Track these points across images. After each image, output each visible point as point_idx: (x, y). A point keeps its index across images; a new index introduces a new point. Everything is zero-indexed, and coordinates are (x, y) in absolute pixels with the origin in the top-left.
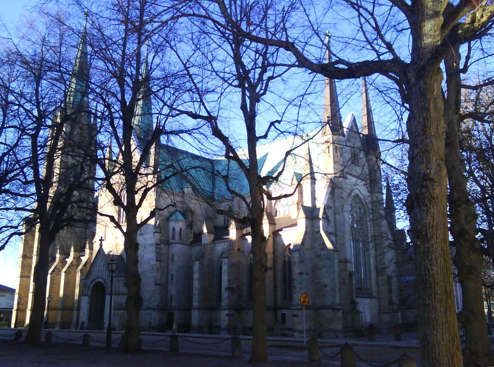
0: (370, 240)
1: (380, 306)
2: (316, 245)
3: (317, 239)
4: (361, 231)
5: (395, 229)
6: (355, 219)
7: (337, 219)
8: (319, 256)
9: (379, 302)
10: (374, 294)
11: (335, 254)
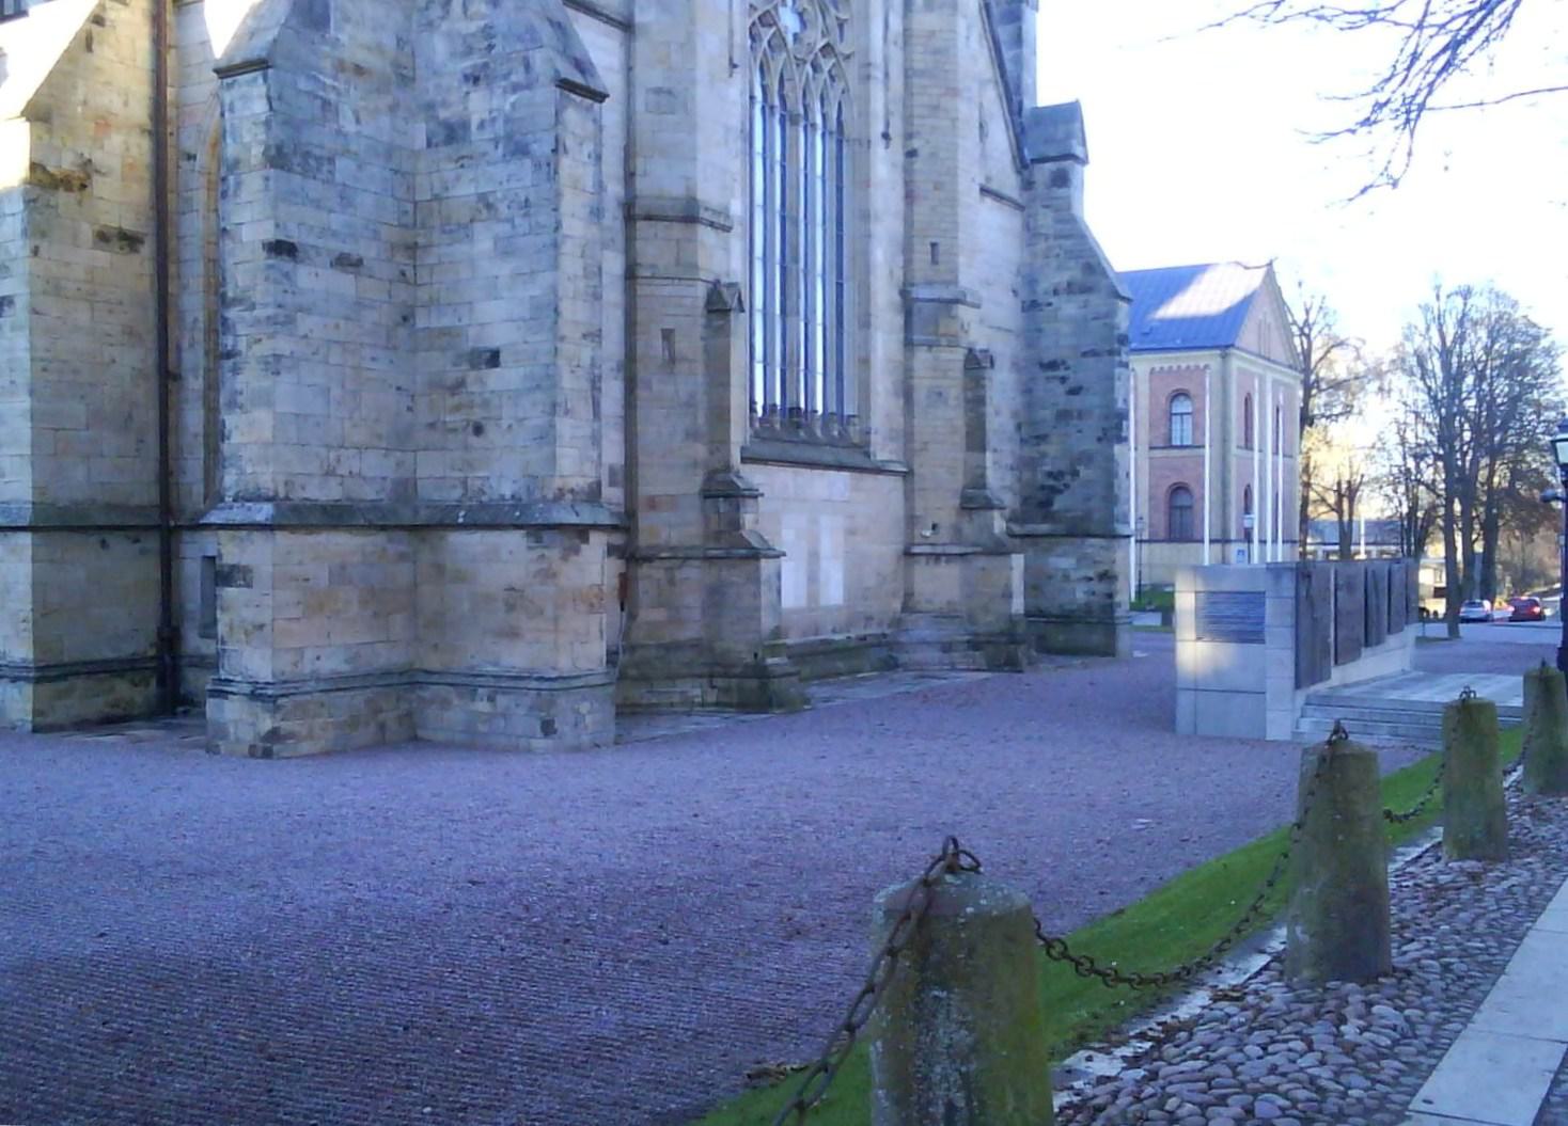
0: (878, 128)
1: (911, 520)
4: (827, 64)
5: (1027, 105)
8: (454, 133)
9: (909, 496)
10: (882, 452)
11: (572, 116)
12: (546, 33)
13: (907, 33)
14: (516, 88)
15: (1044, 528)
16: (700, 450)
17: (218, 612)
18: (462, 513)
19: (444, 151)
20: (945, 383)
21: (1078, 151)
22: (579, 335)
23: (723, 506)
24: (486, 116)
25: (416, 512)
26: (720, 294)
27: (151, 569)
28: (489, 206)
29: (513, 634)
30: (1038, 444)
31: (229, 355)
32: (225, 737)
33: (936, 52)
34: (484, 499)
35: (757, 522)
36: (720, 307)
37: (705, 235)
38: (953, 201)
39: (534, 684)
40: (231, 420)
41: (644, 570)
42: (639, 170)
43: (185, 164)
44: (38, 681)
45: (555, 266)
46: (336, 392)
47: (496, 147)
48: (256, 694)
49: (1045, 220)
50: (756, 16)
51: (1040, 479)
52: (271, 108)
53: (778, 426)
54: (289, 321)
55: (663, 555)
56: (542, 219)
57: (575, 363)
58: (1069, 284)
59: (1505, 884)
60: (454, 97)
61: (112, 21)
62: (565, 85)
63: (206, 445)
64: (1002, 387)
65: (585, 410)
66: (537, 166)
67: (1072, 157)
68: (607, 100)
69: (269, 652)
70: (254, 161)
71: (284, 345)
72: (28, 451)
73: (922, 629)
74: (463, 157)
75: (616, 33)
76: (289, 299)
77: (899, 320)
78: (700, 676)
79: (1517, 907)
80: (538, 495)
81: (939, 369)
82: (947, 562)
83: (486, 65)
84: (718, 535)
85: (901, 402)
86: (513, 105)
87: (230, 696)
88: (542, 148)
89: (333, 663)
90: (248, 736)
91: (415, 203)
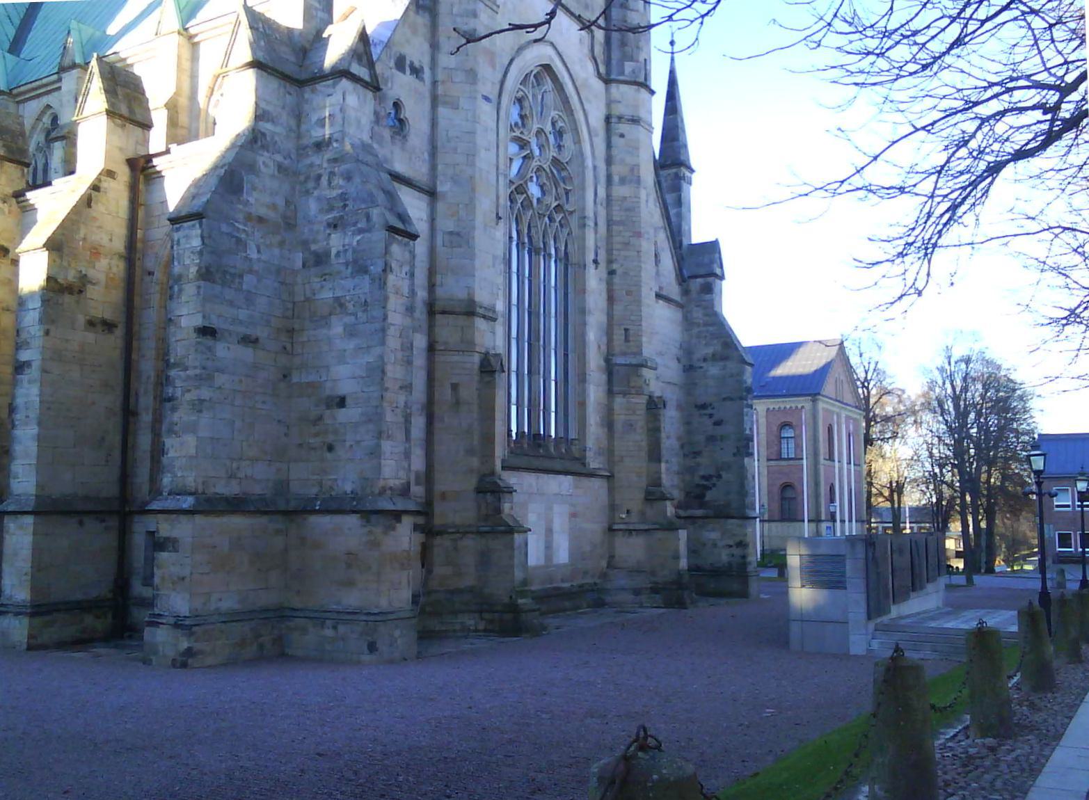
0: (590, 256)
1: (613, 507)
2: (313, 206)
3: (319, 177)
4: (558, 217)
5: (685, 242)
6: (535, 164)
7: (442, 123)
8: (320, 259)
9: (611, 491)
10: (594, 463)
11: (395, 249)
12: (381, 197)
13: (608, 196)
14: (361, 231)
15: (699, 512)
16: (475, 462)
17: (155, 569)
18: (319, 503)
19: (313, 270)
20: (632, 418)
21: (718, 271)
22: (397, 387)
23: (489, 497)
24: (341, 248)
25: (288, 502)
26: (489, 361)
27: (111, 540)
28: (342, 305)
29: (350, 584)
30: (695, 458)
31: (170, 400)
32: (156, 653)
33: (628, 210)
34: (333, 493)
35: (512, 508)
36: (489, 369)
37: (480, 323)
38: (638, 302)
39: (364, 618)
40: (169, 442)
41: (438, 541)
42: (438, 283)
43: (148, 278)
44: (32, 615)
45: (383, 343)
46: (238, 424)
47: (347, 268)
48: (179, 624)
49: (698, 314)
50: (513, 187)
51: (697, 480)
52: (203, 243)
53: (526, 446)
54: (210, 378)
55: (450, 530)
56: (375, 313)
57: (395, 405)
58: (714, 355)
59: (1014, 755)
60: (320, 237)
61: (106, 189)
62: (392, 229)
63: (152, 457)
64: (671, 420)
65: (400, 436)
66: (373, 280)
67: (716, 275)
68: (418, 239)
69: (187, 596)
70: (191, 276)
71: (205, 393)
72: (34, 462)
73: (620, 580)
74: (325, 274)
75: (425, 197)
76: (209, 364)
77: (604, 377)
78: (475, 612)
79: (1023, 770)
80: (368, 491)
81: (630, 409)
82: (637, 535)
83: (342, 217)
84: (486, 518)
85: (606, 430)
86: (358, 241)
87: (161, 626)
88: (376, 269)
89: (229, 604)
90: (171, 654)
91: (294, 303)
